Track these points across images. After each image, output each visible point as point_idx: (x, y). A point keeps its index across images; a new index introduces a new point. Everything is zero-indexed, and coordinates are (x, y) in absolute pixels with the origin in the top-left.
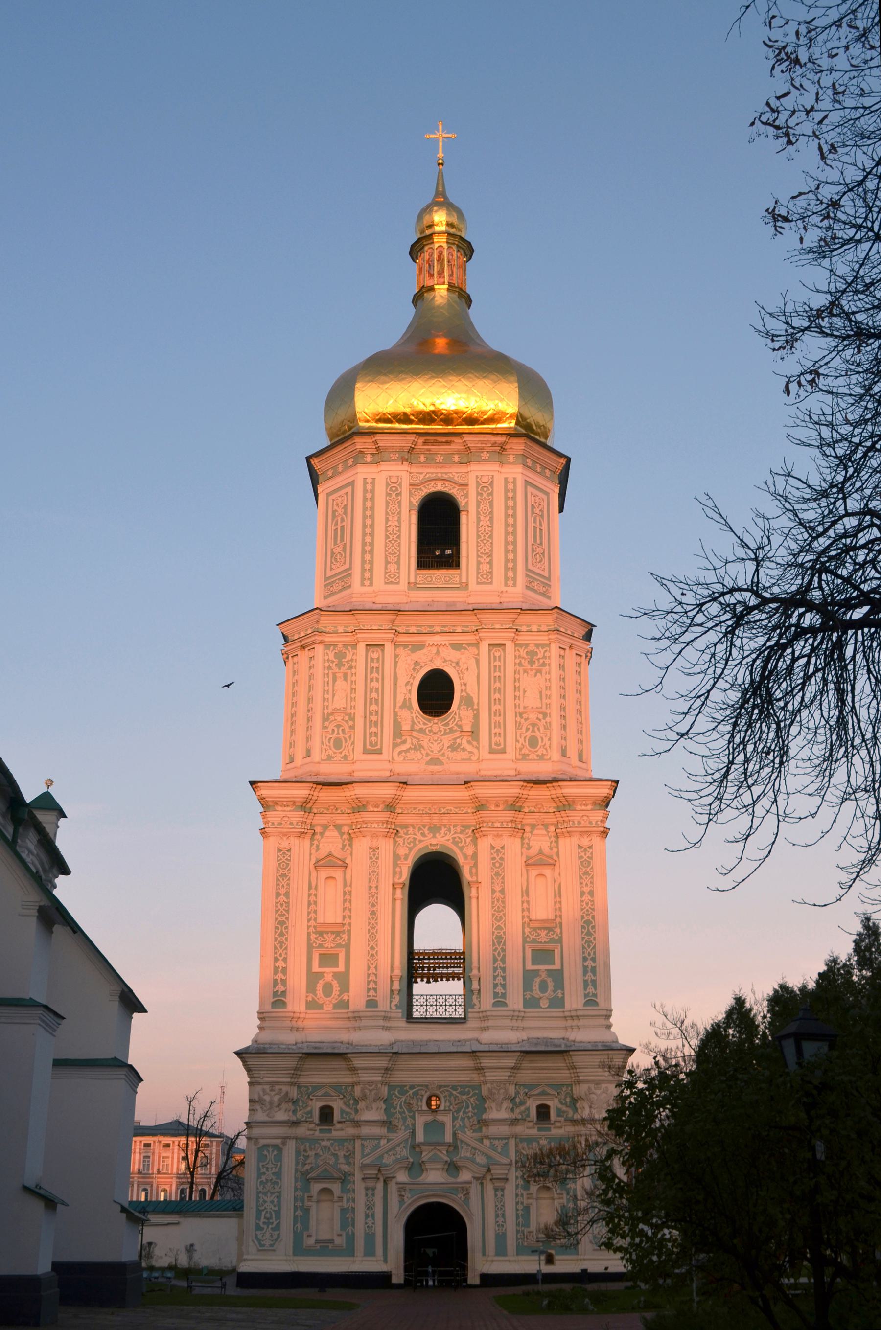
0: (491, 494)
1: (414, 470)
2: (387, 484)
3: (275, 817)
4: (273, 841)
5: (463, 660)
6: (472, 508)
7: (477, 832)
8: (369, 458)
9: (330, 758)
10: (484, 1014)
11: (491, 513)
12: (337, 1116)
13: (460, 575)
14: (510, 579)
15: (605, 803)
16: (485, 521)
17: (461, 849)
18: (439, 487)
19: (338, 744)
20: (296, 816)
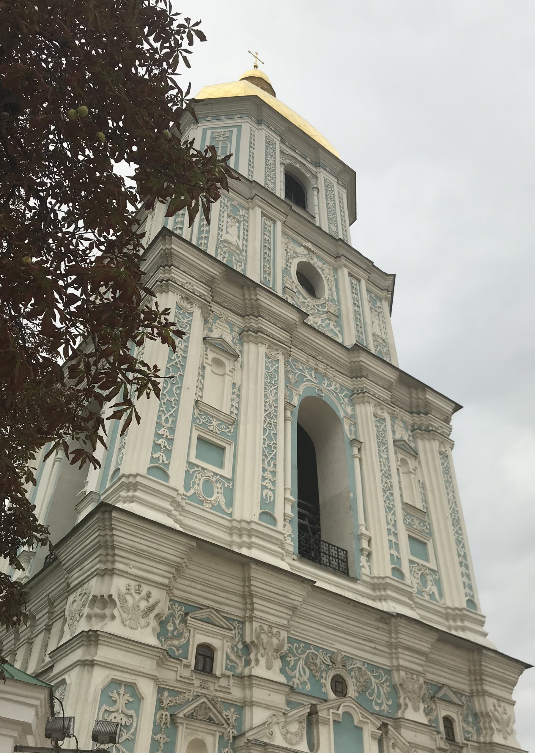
5: (327, 271)
7: (357, 395)
10: (381, 581)
12: (219, 668)
15: (447, 420)
17: (341, 404)
20: (200, 289)
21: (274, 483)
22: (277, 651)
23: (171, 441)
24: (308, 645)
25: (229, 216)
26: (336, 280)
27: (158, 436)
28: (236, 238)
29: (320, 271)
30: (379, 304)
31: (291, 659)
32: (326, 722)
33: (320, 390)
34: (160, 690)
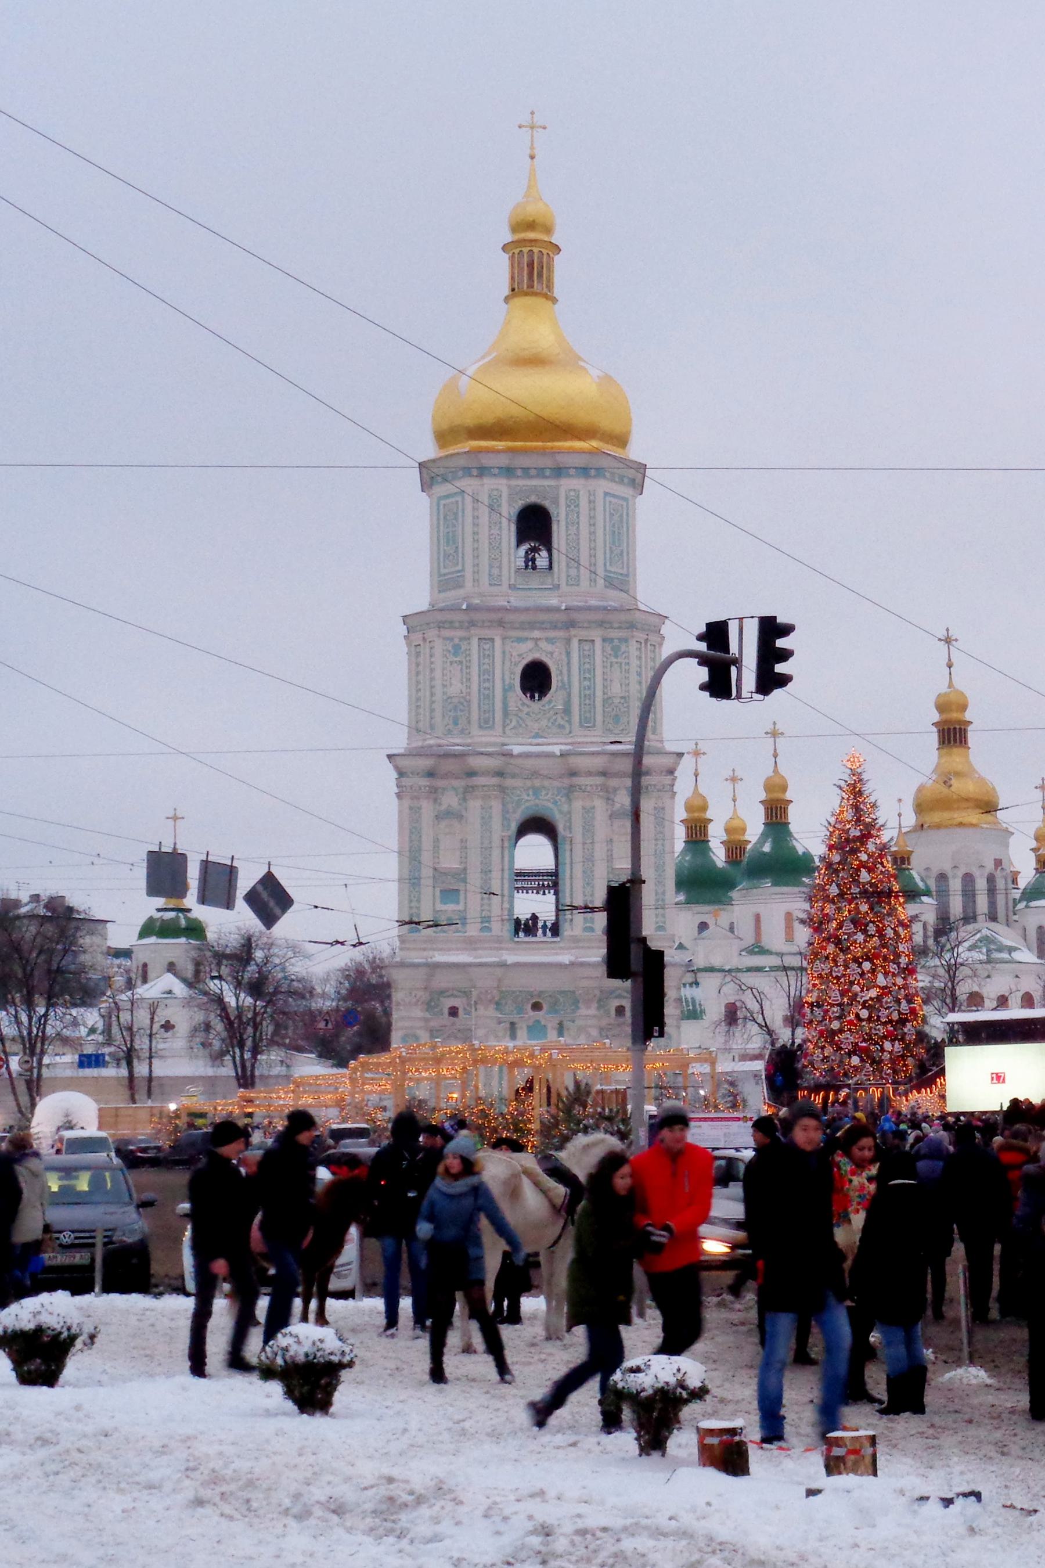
0: (578, 505)
1: (514, 482)
2: (490, 496)
3: (405, 781)
4: (407, 802)
6: (562, 517)
8: (475, 472)
9: (449, 731)
11: (578, 523)
12: (461, 1012)
13: (553, 577)
14: (593, 581)
15: (671, 772)
16: (573, 530)
18: (533, 499)
19: (456, 723)
20: (424, 782)
21: (490, 905)
22: (490, 1001)
23: (418, 908)
24: (514, 992)
25: (451, 663)
26: (568, 654)
27: (411, 908)
28: (460, 685)
29: (545, 659)
30: (623, 648)
31: (503, 1002)
32: (521, 1028)
33: (537, 805)
34: (431, 1031)
